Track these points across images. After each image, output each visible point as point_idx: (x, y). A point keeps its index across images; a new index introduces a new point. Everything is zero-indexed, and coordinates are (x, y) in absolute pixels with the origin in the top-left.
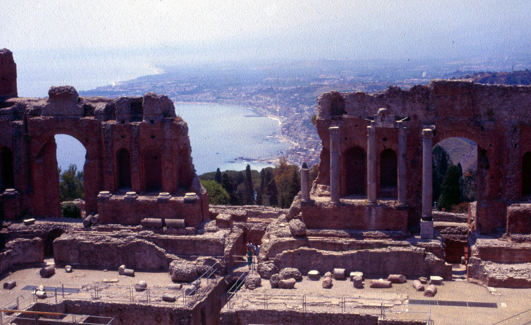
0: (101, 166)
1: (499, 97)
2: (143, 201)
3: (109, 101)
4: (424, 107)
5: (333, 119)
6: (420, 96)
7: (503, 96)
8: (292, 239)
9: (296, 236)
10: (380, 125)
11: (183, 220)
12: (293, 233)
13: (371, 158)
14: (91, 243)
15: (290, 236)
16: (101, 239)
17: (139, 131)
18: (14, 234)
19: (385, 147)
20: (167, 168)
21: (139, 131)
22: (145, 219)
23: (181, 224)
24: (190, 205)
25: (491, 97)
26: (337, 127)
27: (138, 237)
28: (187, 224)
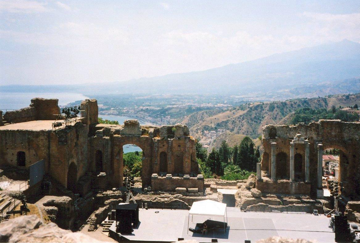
0: (151, 161)
1: (354, 129)
2: (175, 179)
3: (155, 127)
4: (316, 133)
5: (271, 138)
6: (315, 128)
7: (355, 128)
8: (253, 199)
9: (256, 197)
10: (297, 142)
11: (197, 189)
12: (254, 195)
13: (292, 159)
14: (151, 201)
15: (252, 197)
16: (155, 199)
17: (172, 143)
18: (108, 197)
19: (297, 153)
20: (187, 162)
21: (172, 143)
22: (177, 188)
23: (196, 191)
24: (200, 181)
25: (350, 129)
26: (276, 143)
27: (175, 198)
28: (199, 191)
